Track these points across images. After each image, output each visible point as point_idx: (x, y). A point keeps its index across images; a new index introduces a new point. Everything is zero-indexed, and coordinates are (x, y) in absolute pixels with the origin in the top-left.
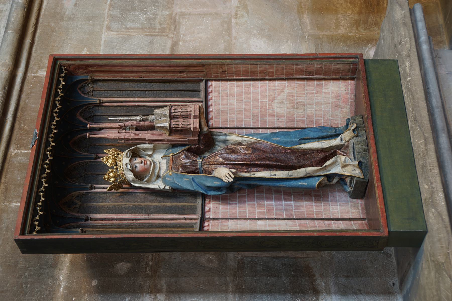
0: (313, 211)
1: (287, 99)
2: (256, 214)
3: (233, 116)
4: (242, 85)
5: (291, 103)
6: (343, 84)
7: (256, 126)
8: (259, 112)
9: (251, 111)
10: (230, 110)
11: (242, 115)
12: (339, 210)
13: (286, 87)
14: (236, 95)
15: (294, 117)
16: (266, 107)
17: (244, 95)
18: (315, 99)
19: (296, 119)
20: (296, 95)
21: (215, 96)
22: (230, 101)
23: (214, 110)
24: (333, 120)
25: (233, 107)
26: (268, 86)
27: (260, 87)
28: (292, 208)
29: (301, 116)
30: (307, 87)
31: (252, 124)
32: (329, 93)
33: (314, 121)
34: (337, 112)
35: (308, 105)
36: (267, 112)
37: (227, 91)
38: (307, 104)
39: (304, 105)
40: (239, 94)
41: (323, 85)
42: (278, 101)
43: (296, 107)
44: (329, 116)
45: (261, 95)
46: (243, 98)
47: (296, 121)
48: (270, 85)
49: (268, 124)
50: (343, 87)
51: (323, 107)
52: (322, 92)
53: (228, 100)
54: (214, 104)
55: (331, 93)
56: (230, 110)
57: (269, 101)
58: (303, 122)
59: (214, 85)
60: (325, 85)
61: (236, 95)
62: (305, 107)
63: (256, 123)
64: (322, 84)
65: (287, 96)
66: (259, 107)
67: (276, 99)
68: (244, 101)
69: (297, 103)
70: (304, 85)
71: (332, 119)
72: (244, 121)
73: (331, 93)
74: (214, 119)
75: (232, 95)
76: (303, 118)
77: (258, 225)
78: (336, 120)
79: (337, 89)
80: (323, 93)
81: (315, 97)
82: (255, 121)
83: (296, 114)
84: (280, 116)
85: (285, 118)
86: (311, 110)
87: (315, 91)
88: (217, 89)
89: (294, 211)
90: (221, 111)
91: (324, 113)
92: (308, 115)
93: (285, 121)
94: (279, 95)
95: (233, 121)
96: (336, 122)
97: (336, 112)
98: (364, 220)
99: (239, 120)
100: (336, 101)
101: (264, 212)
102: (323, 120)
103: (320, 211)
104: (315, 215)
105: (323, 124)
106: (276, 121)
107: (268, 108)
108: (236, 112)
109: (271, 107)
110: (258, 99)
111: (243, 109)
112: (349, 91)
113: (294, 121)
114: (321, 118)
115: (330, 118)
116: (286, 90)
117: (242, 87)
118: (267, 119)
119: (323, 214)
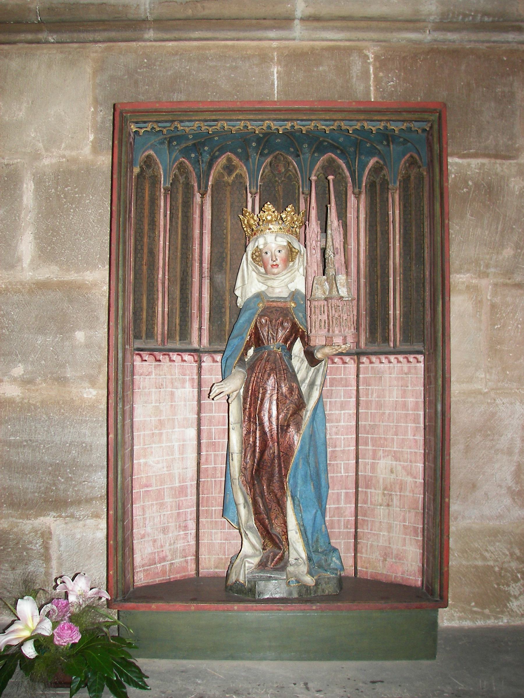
0: (213, 507)
1: (397, 479)
2: (208, 427)
3: (375, 395)
4: (418, 411)
5: (391, 486)
6: (417, 568)
7: (361, 429)
8: (379, 435)
9: (381, 423)
10: (383, 390)
11: (376, 409)
12: (215, 541)
13: (414, 480)
14: (403, 400)
15: (371, 489)
16: (387, 447)
17: (403, 412)
18: (396, 522)
19: (369, 490)
20: (402, 494)
21: (402, 367)
22: (395, 391)
23: (382, 365)
24: (367, 547)
25: (387, 395)
26: (416, 451)
27: (415, 439)
28: (218, 478)
29: (373, 500)
30: (413, 514)
31: (363, 423)
32: (405, 546)
33: (366, 518)
34: (378, 554)
35: (387, 511)
36: (380, 448)
37: (409, 385)
38: (389, 510)
39: (388, 505)
40: (404, 406)
41: (417, 538)
42: (394, 465)
43: (385, 492)
44: (372, 541)
45: (403, 439)
46: (399, 412)
47: (367, 490)
48: (418, 454)
49: (363, 447)
50: (413, 568)
51: (385, 533)
52: (406, 535)
53: (396, 388)
54: (391, 365)
55: (404, 548)
56: (383, 390)
57: (395, 452)
58: (365, 502)
59: (418, 365)
60: (417, 541)
61: (403, 400)
62: (386, 506)
63: (365, 430)
64: (418, 537)
65: (401, 480)
66: (387, 435)
67: (398, 463)
68: (395, 412)
69: (391, 495)
70: (417, 508)
71: (369, 545)
72: (366, 411)
73: (404, 548)
74: (371, 365)
75: (404, 394)
76: (371, 501)
77: (183, 429)
78: (367, 551)
79: (410, 557)
80: (404, 536)
81: (398, 523)
82: (368, 428)
83: (375, 491)
84: (373, 467)
85: (371, 475)
86: (382, 515)
87: (407, 524)
88: (413, 371)
89: (213, 480)
90: (381, 377)
91: (377, 534)
92: (373, 510)
93: (366, 474)
94: (403, 467)
95: (367, 395)
96: (364, 550)
97: (378, 552)
98: (198, 573)
99: (368, 404)
100: (392, 555)
101: (211, 438)
102: (367, 531)
103: (212, 516)
104: (206, 508)
105: (362, 530)
106: (367, 461)
107: (384, 449)
108: (379, 399)
109: (386, 454)
110: (397, 435)
111: (384, 410)
112: (406, 576)
113: (366, 488)
114: (369, 529)
115: (370, 542)
116: (409, 479)
117: (415, 411)
118: (370, 447)
119: (207, 520)
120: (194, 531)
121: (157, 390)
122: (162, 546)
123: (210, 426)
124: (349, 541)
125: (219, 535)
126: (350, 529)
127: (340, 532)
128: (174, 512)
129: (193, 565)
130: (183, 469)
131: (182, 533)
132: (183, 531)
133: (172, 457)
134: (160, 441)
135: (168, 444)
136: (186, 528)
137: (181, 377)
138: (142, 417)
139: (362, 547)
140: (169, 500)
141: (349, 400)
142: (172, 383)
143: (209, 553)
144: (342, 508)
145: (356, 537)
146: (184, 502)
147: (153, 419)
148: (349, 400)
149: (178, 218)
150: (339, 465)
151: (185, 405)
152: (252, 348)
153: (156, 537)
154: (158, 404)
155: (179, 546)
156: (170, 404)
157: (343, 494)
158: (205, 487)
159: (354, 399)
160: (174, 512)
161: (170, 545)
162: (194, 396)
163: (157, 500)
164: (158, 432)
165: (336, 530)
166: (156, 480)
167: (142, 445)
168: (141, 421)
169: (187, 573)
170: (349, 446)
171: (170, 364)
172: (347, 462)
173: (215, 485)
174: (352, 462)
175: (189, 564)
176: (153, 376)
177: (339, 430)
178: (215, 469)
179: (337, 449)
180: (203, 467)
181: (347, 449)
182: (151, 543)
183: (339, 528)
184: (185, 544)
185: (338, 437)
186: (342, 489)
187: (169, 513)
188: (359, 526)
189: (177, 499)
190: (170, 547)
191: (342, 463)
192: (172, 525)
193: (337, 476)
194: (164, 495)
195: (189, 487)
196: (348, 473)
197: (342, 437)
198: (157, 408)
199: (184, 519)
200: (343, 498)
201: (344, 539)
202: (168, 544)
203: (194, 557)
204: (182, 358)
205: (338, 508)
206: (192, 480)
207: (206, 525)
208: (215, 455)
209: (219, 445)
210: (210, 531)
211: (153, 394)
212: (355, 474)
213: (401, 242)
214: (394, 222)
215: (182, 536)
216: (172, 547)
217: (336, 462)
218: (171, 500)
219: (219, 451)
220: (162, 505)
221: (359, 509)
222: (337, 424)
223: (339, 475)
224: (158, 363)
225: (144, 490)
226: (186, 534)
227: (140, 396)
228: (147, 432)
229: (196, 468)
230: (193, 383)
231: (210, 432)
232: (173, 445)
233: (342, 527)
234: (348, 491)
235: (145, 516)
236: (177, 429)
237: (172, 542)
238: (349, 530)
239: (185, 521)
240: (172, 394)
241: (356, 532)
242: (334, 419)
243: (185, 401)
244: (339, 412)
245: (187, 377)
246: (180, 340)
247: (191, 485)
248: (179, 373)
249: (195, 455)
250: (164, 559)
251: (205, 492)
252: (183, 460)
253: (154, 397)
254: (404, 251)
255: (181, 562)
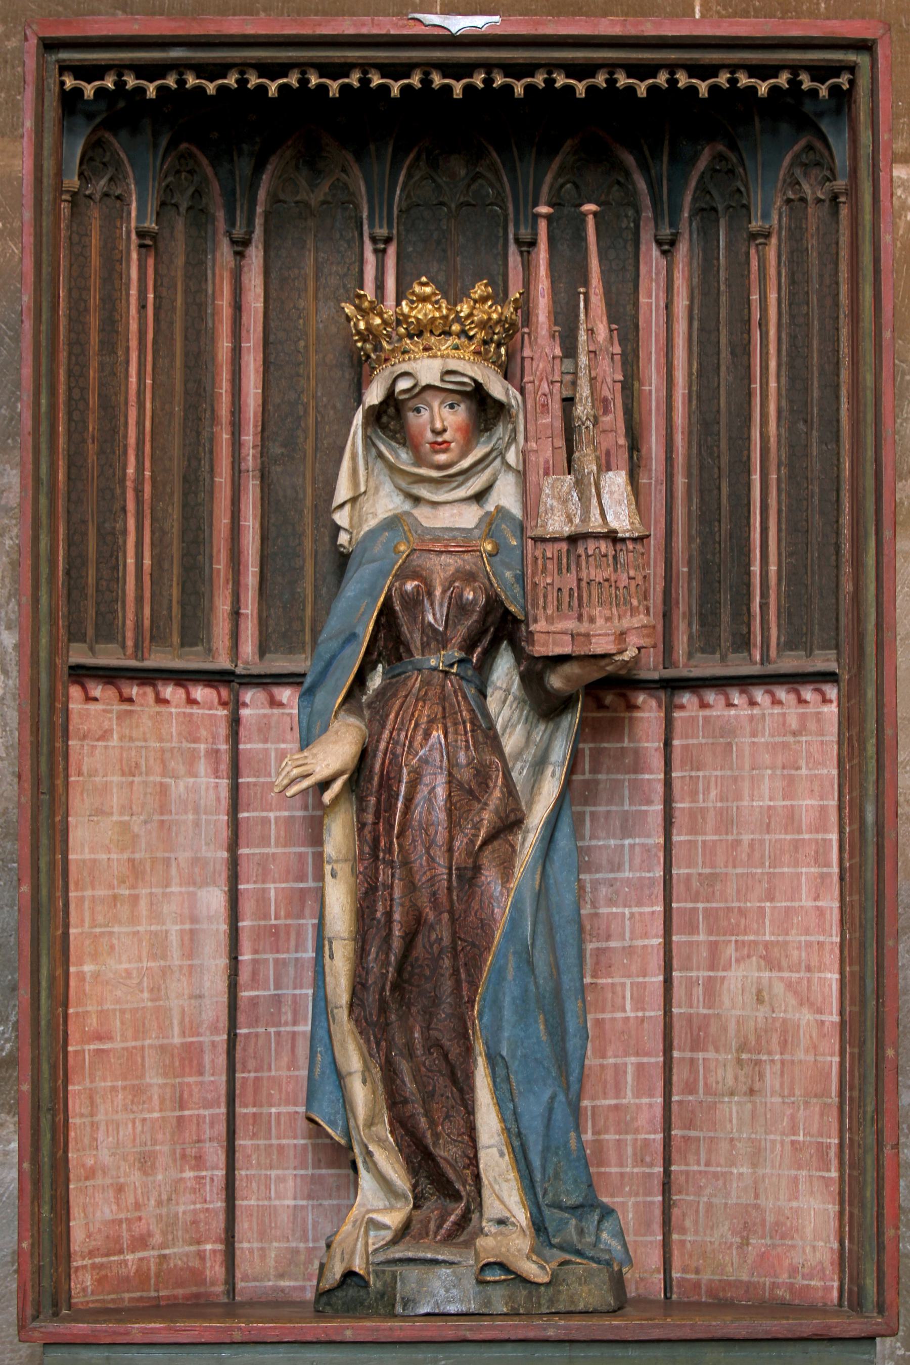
2: (259, 886)
12: (277, 1202)
28: (286, 1024)
77: (191, 889)
89: (272, 1030)
96: (688, 1223)
101: (266, 916)
104: (254, 1110)
120: (221, 1173)
121: (124, 779)
122: (137, 1206)
123: (264, 882)
124: (649, 1199)
125: (291, 1183)
126: (651, 1165)
127: (622, 1175)
128: (168, 1114)
129: (217, 1268)
130: (191, 997)
131: (189, 1174)
132: (192, 1169)
133: (162, 963)
134: (134, 920)
135: (153, 928)
136: (199, 1161)
137: (185, 745)
138: (87, 850)
139: (684, 1215)
140: (154, 1081)
141: (644, 808)
142: (163, 761)
143: (262, 1235)
144: (627, 1107)
145: (667, 1187)
146: (195, 1090)
147: (114, 856)
148: (644, 808)
149: (174, 309)
150: (619, 989)
151: (197, 824)
152: (380, 668)
153: (122, 1180)
154: (127, 818)
155: (181, 1209)
156: (156, 817)
157: (630, 1070)
158: (251, 1050)
159: (658, 807)
160: (168, 1114)
161: (159, 1203)
162: (218, 799)
163: (125, 1079)
164: (127, 892)
165: (613, 1170)
166: (123, 1023)
167: (87, 924)
168: (84, 861)
169: (202, 1290)
170: (646, 935)
171: (158, 709)
172: (641, 979)
173: (278, 1043)
174: (654, 979)
175: (208, 1265)
176: (115, 741)
177: (617, 893)
178: (277, 1000)
179: (613, 944)
180: (245, 994)
181: (640, 943)
182: (111, 1194)
183: (621, 1165)
184: (198, 1206)
185: (614, 910)
186: (626, 1054)
187: (156, 1115)
188: (675, 1156)
189: (178, 1080)
190: (158, 1211)
191: (628, 982)
192: (163, 1149)
193: (613, 1019)
194: (143, 1066)
195: (207, 1048)
196: (643, 1009)
197: (627, 911)
198: (124, 827)
199: (195, 1138)
200: (629, 1078)
201: (637, 1195)
202: (152, 1202)
203: (220, 1247)
204: (188, 693)
205: (616, 1107)
206: (215, 1030)
207: (254, 1157)
208: (276, 961)
209: (288, 933)
210: (263, 1172)
211: (115, 790)
212: (661, 1013)
213: (783, 380)
214: (763, 324)
215: (189, 1184)
216: (164, 1211)
217: (610, 980)
218: (160, 1081)
219: (288, 951)
220: (138, 1092)
221: (675, 1108)
222: (612, 875)
223: (620, 1015)
224: (126, 707)
225: (92, 1047)
226: (199, 1179)
227: (82, 794)
228: (101, 892)
229: (225, 999)
230: (217, 762)
231: (262, 898)
232: (167, 932)
233: (630, 1161)
234: (645, 1060)
235: (96, 1119)
236: (174, 889)
237: (164, 1197)
238: (647, 1170)
239: (199, 1141)
240: (163, 790)
241: (667, 1173)
242: (604, 862)
243: (196, 811)
244: (619, 842)
245: (202, 747)
246: (183, 645)
247: (214, 1044)
248: (179, 734)
249: (223, 962)
250: (141, 1242)
251: (251, 1064)
252: (190, 973)
253: (115, 800)
254: (791, 402)
255: (187, 1255)
